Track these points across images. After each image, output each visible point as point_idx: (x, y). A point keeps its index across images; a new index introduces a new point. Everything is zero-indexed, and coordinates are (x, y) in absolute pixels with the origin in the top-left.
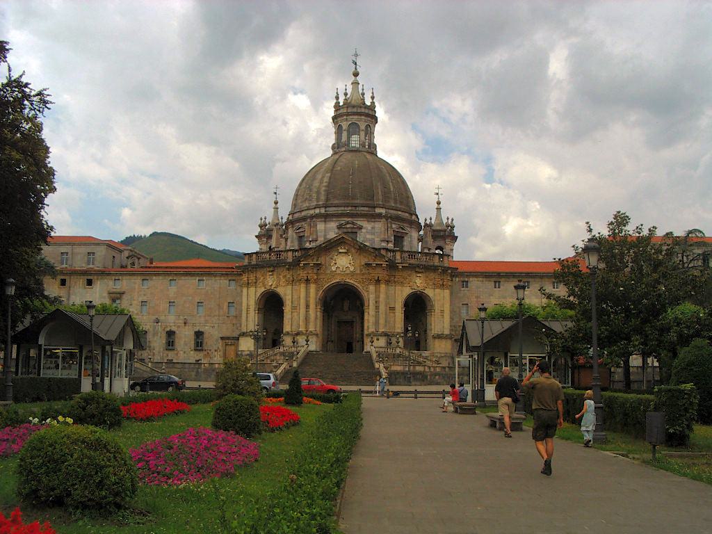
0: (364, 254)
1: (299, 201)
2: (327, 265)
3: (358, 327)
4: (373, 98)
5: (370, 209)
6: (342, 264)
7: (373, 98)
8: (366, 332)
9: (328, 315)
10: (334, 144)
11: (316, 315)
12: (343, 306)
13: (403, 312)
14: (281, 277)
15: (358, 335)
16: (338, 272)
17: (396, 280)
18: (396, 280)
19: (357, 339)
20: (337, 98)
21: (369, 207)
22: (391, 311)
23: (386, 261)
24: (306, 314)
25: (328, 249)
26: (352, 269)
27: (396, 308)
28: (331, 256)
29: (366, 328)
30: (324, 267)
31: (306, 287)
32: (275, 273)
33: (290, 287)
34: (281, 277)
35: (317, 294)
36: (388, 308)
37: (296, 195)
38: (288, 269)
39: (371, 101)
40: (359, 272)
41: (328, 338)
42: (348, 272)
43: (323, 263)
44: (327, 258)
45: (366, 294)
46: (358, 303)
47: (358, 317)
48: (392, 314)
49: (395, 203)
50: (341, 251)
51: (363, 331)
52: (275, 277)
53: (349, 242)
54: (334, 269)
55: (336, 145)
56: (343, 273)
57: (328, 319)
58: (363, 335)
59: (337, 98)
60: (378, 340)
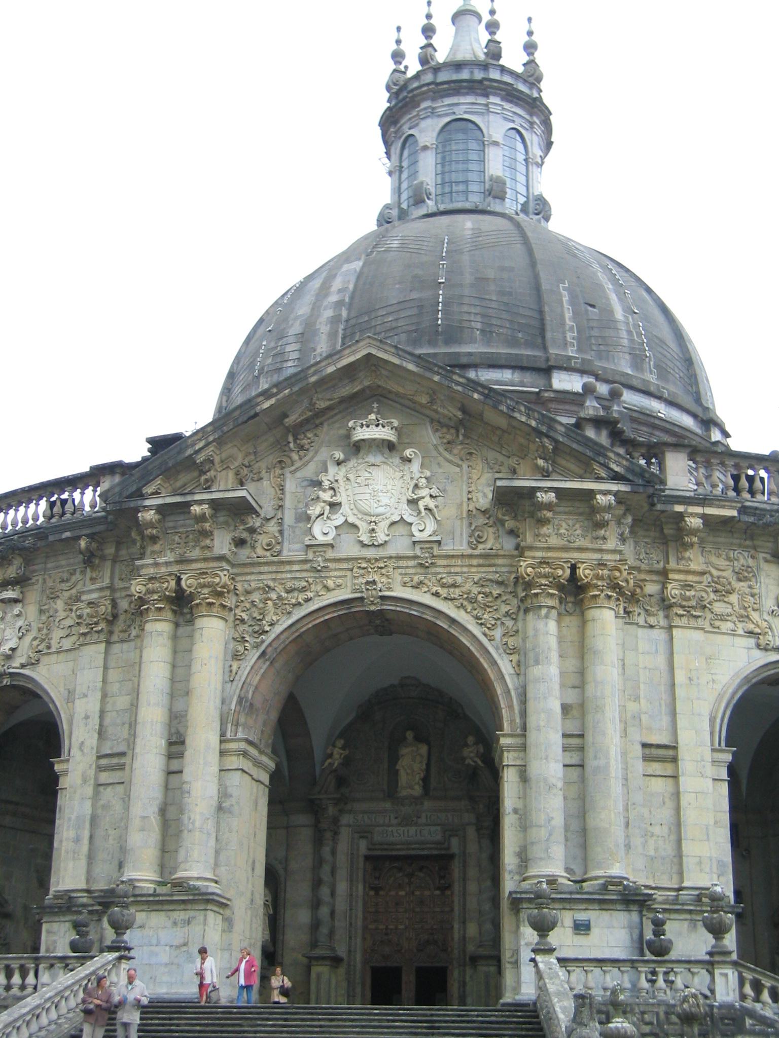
0: (491, 455)
1: (237, 390)
2: (289, 518)
3: (472, 872)
4: (530, 48)
5: (528, 377)
6: (374, 508)
7: (530, 48)
8: (509, 884)
9: (318, 821)
10: (387, 207)
11: (224, 794)
12: (393, 775)
13: (724, 774)
14: (60, 604)
15: (472, 930)
16: (348, 548)
17: (673, 590)
18: (673, 590)
19: (471, 948)
20: (398, 56)
21: (523, 368)
22: (656, 768)
23: (616, 477)
24: (167, 788)
25: (297, 430)
26: (425, 529)
27: (684, 754)
28: (309, 471)
29: (509, 858)
30: (272, 527)
31: (175, 638)
32: (33, 595)
33: (94, 652)
34: (60, 604)
35: (230, 677)
36: (638, 750)
37: (231, 375)
38: (90, 560)
39: (525, 58)
40: (462, 547)
41: (314, 944)
42: (400, 546)
43: (267, 509)
44: (291, 485)
45: (506, 665)
46: (471, 754)
47: (471, 832)
48: (660, 786)
49: (638, 360)
50: (362, 434)
51: (496, 879)
52: (31, 611)
53: (407, 389)
54: (322, 531)
55: (395, 213)
56: (370, 553)
57: (318, 842)
58: (495, 900)
59: (398, 56)
60: (582, 928)
